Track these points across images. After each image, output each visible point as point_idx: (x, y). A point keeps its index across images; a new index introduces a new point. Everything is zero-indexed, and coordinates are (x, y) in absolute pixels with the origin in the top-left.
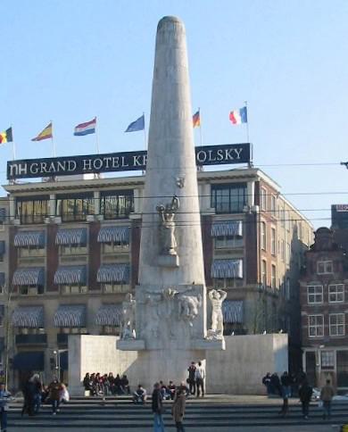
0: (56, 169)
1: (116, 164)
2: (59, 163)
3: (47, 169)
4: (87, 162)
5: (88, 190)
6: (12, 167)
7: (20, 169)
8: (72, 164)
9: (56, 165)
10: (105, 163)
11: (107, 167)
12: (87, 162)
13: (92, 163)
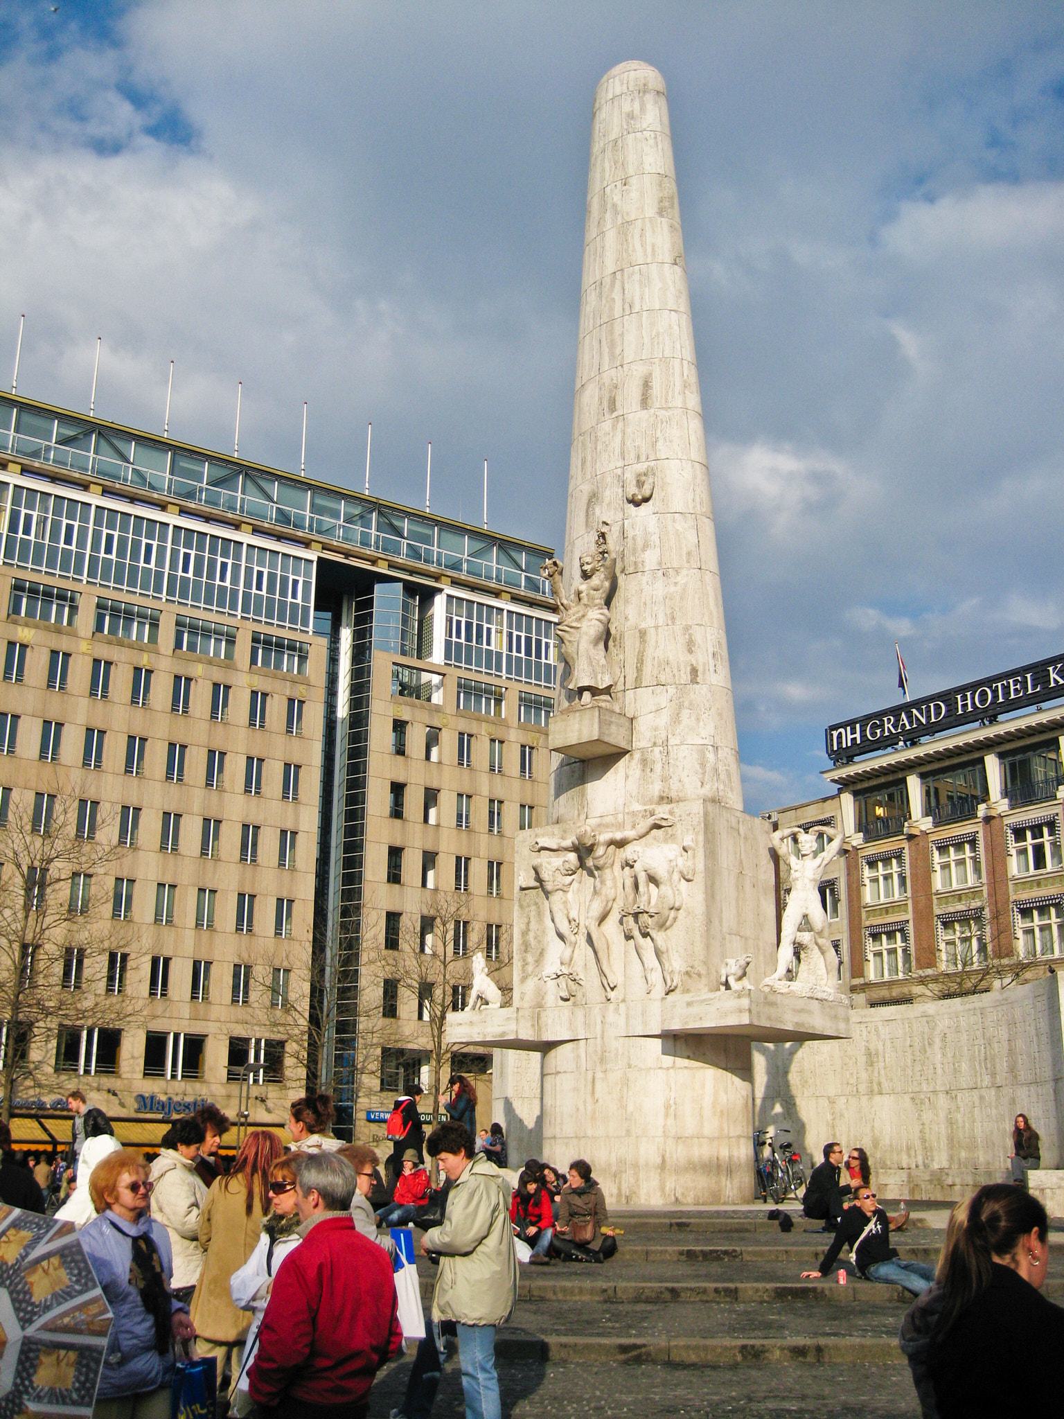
0: (911, 723)
1: (1016, 690)
2: (915, 711)
3: (895, 727)
4: (964, 698)
5: (976, 755)
6: (835, 734)
7: (848, 737)
8: (938, 707)
9: (910, 716)
10: (995, 692)
11: (1001, 700)
12: (964, 698)
13: (973, 698)
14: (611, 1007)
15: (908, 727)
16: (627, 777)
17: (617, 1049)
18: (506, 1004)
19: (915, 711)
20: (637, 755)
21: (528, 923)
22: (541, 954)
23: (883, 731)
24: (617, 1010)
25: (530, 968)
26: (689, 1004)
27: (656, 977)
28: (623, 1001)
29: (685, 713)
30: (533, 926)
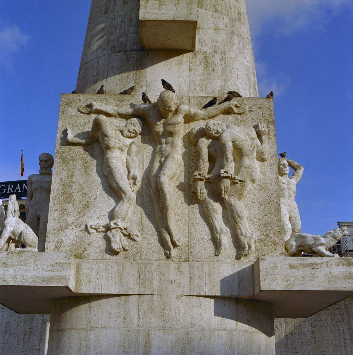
0: (21, 190)
2: (24, 185)
3: (13, 190)
14: (173, 265)
15: (20, 191)
16: (191, 70)
17: (178, 307)
18: (42, 248)
19: (24, 185)
20: (200, 57)
21: (72, 176)
22: (87, 206)
23: (7, 191)
24: (179, 269)
25: (71, 219)
26: (292, 267)
27: (226, 239)
28: (187, 260)
29: (236, 40)
30: (78, 177)
